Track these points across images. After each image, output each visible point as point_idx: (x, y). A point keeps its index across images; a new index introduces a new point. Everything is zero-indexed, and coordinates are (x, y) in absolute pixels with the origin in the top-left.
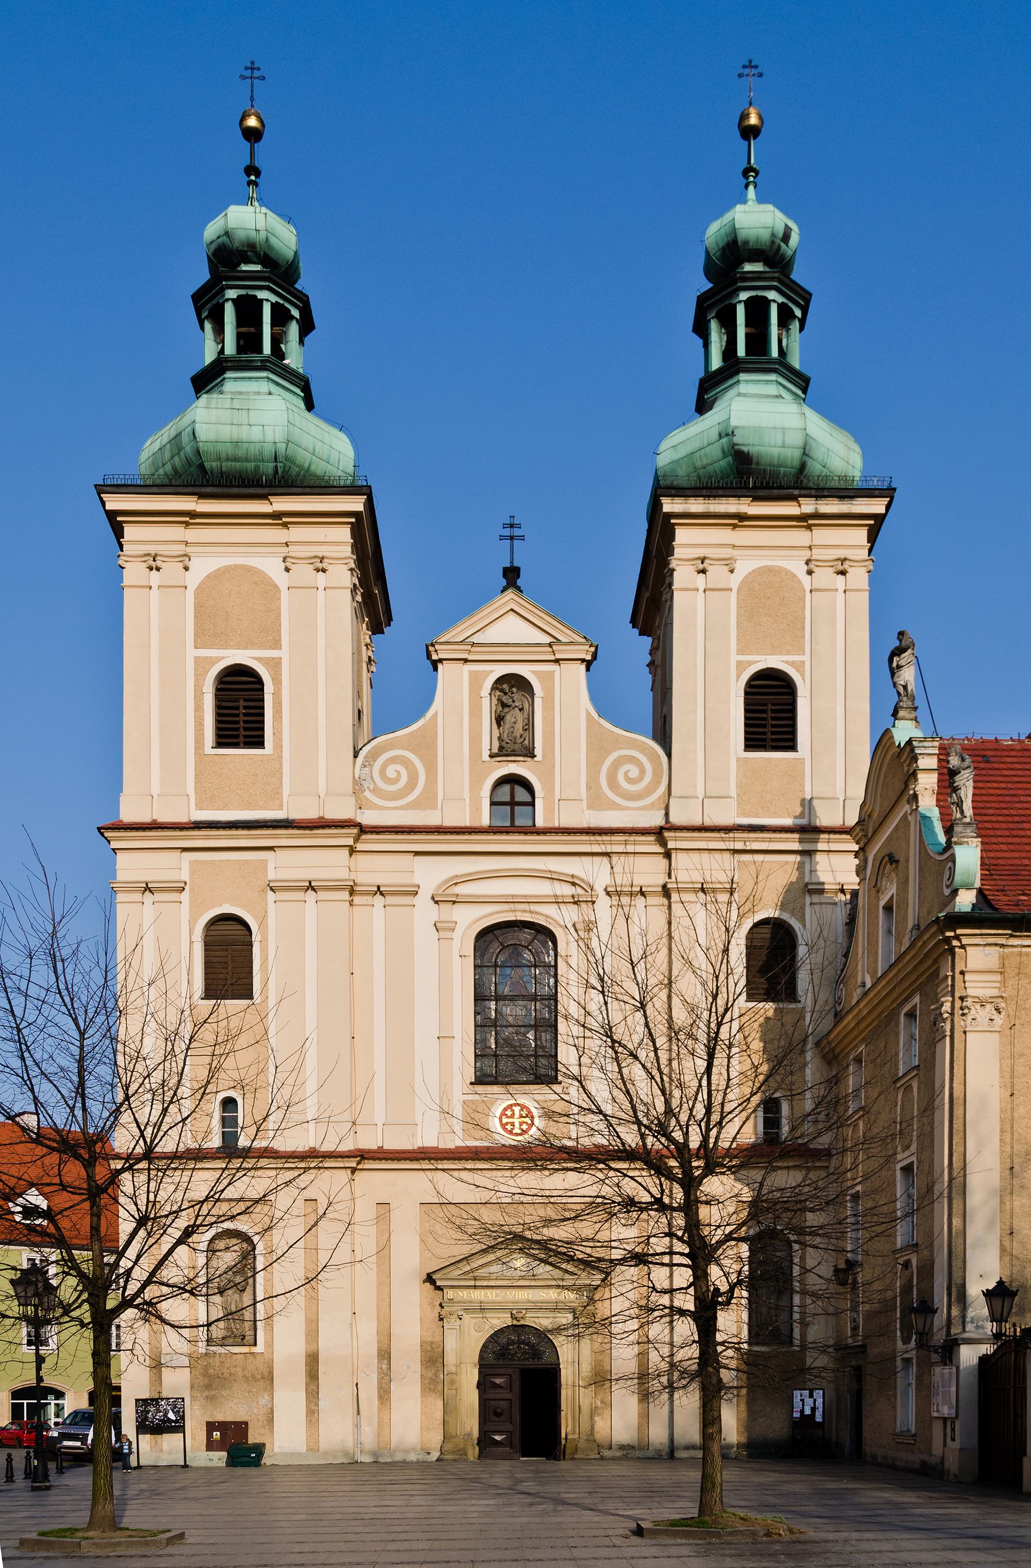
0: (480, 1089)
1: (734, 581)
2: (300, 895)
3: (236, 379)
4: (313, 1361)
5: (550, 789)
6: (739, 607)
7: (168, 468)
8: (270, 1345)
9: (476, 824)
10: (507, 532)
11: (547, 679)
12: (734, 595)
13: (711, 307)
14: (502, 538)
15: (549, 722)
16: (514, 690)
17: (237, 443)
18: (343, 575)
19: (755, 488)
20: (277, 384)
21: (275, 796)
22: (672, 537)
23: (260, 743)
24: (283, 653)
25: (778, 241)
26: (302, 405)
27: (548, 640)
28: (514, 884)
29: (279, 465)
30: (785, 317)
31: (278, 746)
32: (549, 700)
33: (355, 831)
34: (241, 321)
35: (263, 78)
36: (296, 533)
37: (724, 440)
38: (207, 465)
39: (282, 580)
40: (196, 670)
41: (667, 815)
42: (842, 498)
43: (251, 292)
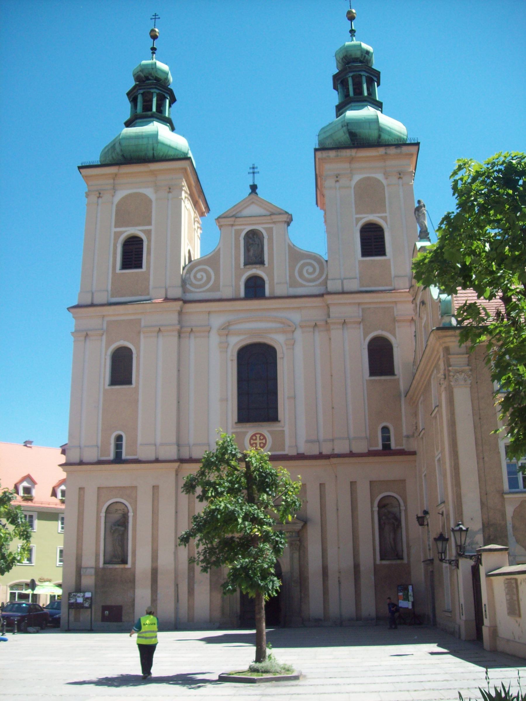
0: (240, 425)
3: (140, 122)
4: (155, 572)
5: (272, 279)
7: (111, 158)
8: (134, 563)
10: (251, 171)
11: (270, 231)
15: (271, 248)
23: (140, 266)
24: (152, 227)
25: (364, 54)
28: (256, 323)
29: (155, 152)
31: (148, 268)
32: (271, 239)
34: (145, 101)
35: (159, 18)
41: (327, 288)
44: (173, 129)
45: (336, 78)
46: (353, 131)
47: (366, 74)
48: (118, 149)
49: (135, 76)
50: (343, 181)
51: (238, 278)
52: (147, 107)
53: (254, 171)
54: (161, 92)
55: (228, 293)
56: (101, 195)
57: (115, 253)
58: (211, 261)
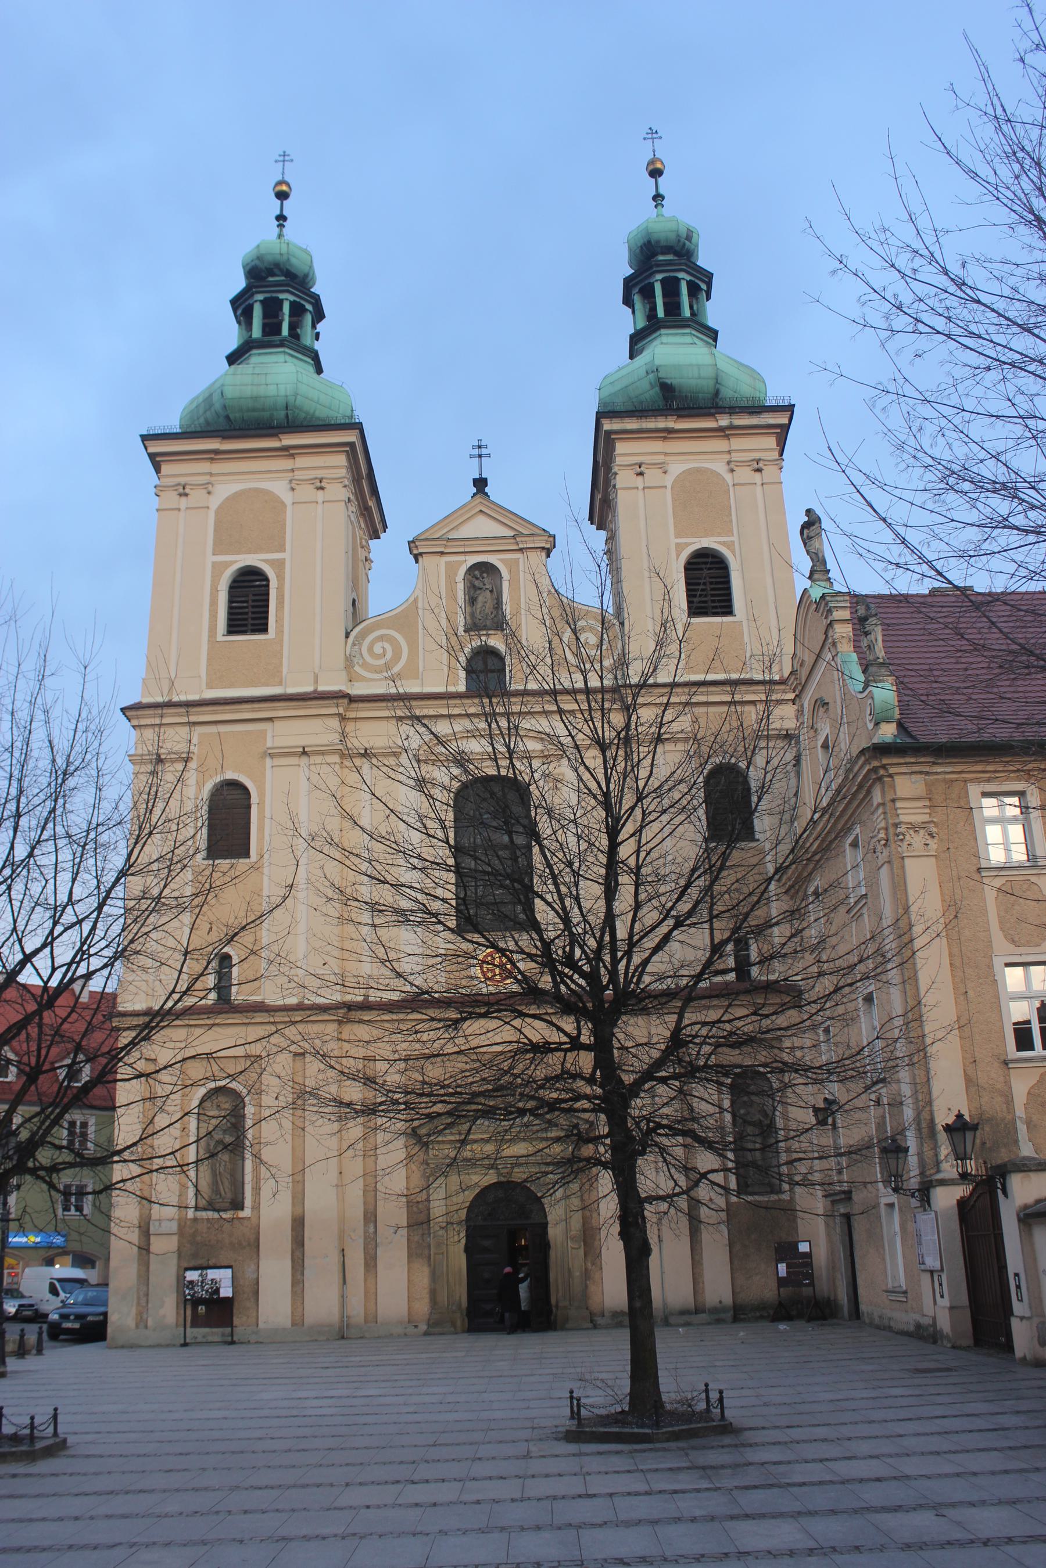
1: (669, 480)
2: (294, 760)
3: (259, 354)
4: (298, 1224)
6: (674, 500)
7: (202, 420)
8: (256, 1207)
10: (476, 452)
11: (512, 566)
12: (669, 491)
13: (635, 285)
16: (485, 575)
18: (340, 492)
19: (678, 409)
20: (292, 356)
21: (275, 675)
22: (613, 449)
23: (264, 629)
25: (683, 240)
26: (311, 369)
27: (511, 533)
29: (290, 412)
30: (694, 290)
31: (280, 631)
33: (346, 701)
34: (266, 316)
36: (301, 461)
37: (651, 376)
38: (231, 416)
39: (287, 497)
40: (212, 573)
42: (751, 413)
43: (274, 295)
45: (629, 284)
46: (669, 382)
47: (688, 278)
48: (218, 406)
49: (248, 268)
50: (652, 476)
53: (480, 452)
56: (187, 491)
57: (214, 603)
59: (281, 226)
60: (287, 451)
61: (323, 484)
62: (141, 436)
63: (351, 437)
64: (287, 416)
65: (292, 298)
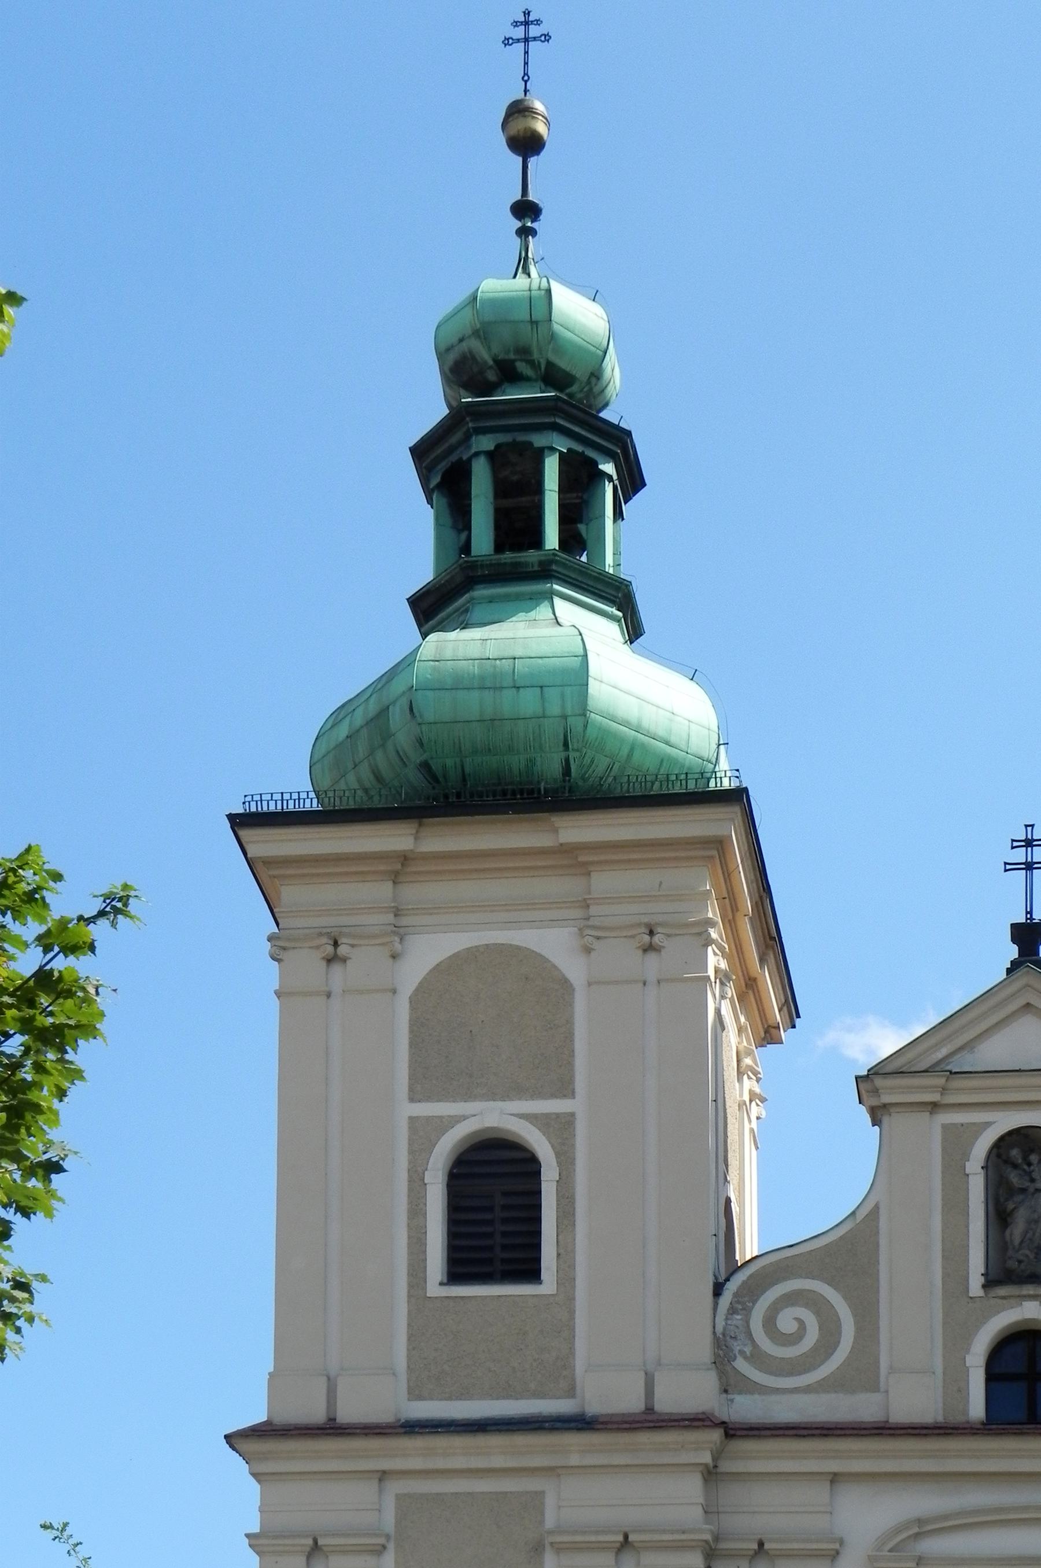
3: (491, 600)
9: (958, 1419)
10: (1020, 855)
14: (1009, 867)
17: (493, 722)
23: (531, 1273)
29: (572, 755)
34: (502, 489)
35: (546, 37)
36: (603, 882)
39: (574, 968)
43: (522, 437)
44: (634, 631)
48: (403, 734)
49: (452, 357)
51: (957, 1339)
52: (518, 527)
54: (579, 448)
55: (914, 1399)
56: (343, 950)
58: (847, 1257)
59: (524, 233)
60: (574, 859)
61: (656, 939)
62: (231, 817)
63: (725, 823)
64: (567, 771)
65: (563, 444)
